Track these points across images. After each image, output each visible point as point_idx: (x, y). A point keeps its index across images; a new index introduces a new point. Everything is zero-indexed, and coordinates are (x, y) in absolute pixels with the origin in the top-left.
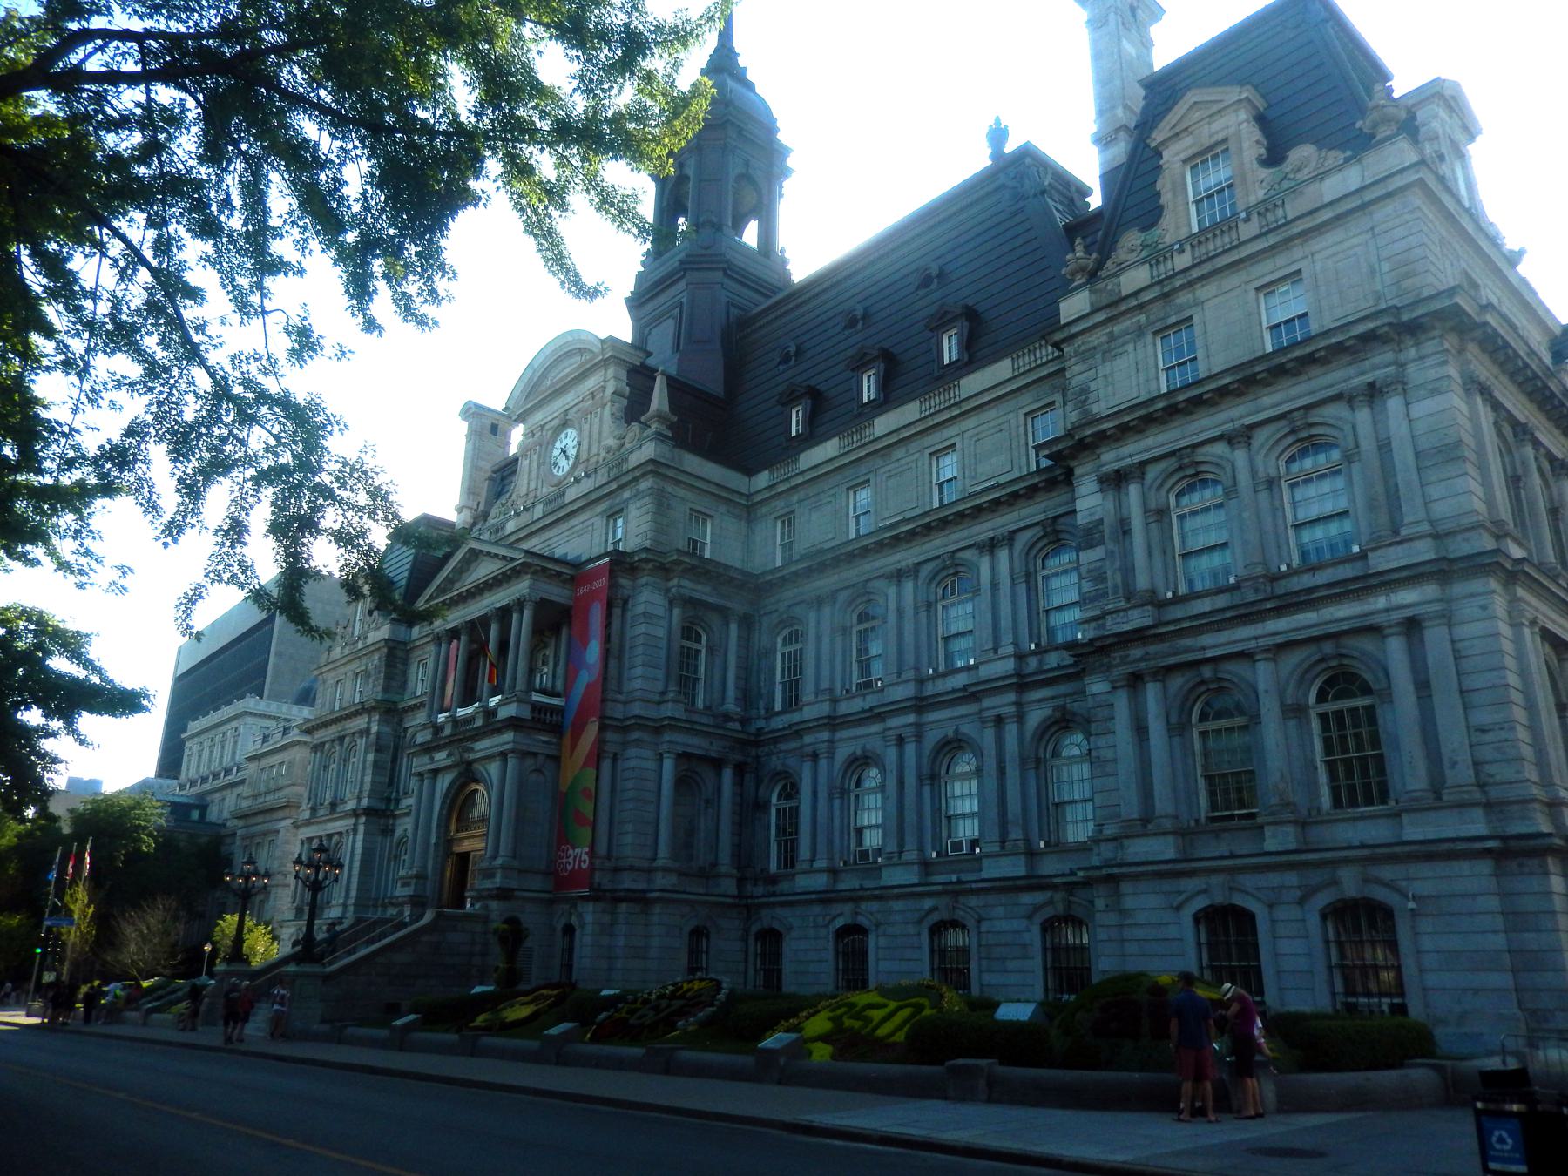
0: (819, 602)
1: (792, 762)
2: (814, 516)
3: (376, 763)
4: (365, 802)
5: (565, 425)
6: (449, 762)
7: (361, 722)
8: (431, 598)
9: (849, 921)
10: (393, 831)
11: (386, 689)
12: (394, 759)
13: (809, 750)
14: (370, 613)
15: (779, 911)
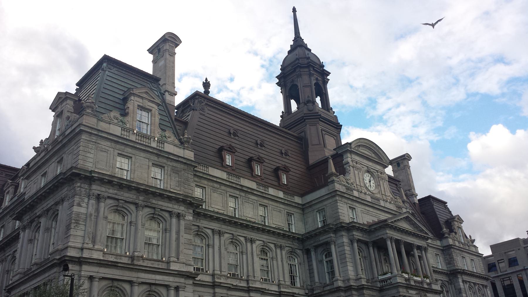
5: (368, 172)
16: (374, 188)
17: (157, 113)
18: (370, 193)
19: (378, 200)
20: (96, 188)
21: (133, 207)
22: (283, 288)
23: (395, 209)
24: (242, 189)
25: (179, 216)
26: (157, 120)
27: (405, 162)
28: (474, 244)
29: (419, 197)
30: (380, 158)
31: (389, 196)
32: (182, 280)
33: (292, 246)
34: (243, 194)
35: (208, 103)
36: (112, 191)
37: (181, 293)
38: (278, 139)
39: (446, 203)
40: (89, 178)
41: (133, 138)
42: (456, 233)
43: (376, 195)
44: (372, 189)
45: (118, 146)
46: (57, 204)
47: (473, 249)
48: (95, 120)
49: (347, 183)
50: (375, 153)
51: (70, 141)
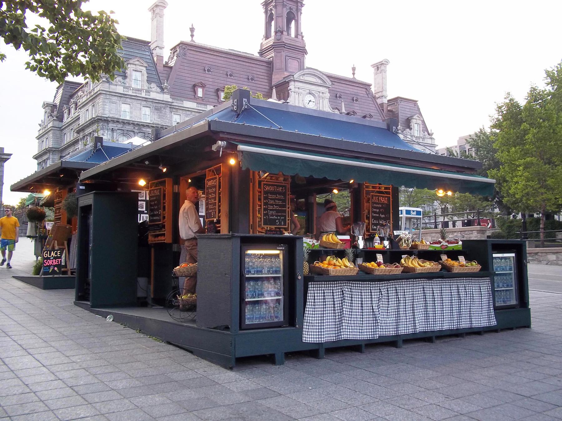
17: (145, 73)
20: (111, 125)
21: (132, 133)
26: (146, 78)
27: (383, 67)
28: (433, 136)
29: (388, 98)
36: (120, 126)
39: (417, 101)
40: (106, 121)
41: (130, 93)
42: (411, 129)
45: (122, 99)
46: (93, 131)
47: (429, 141)
48: (107, 85)
50: (319, 78)
51: (96, 96)
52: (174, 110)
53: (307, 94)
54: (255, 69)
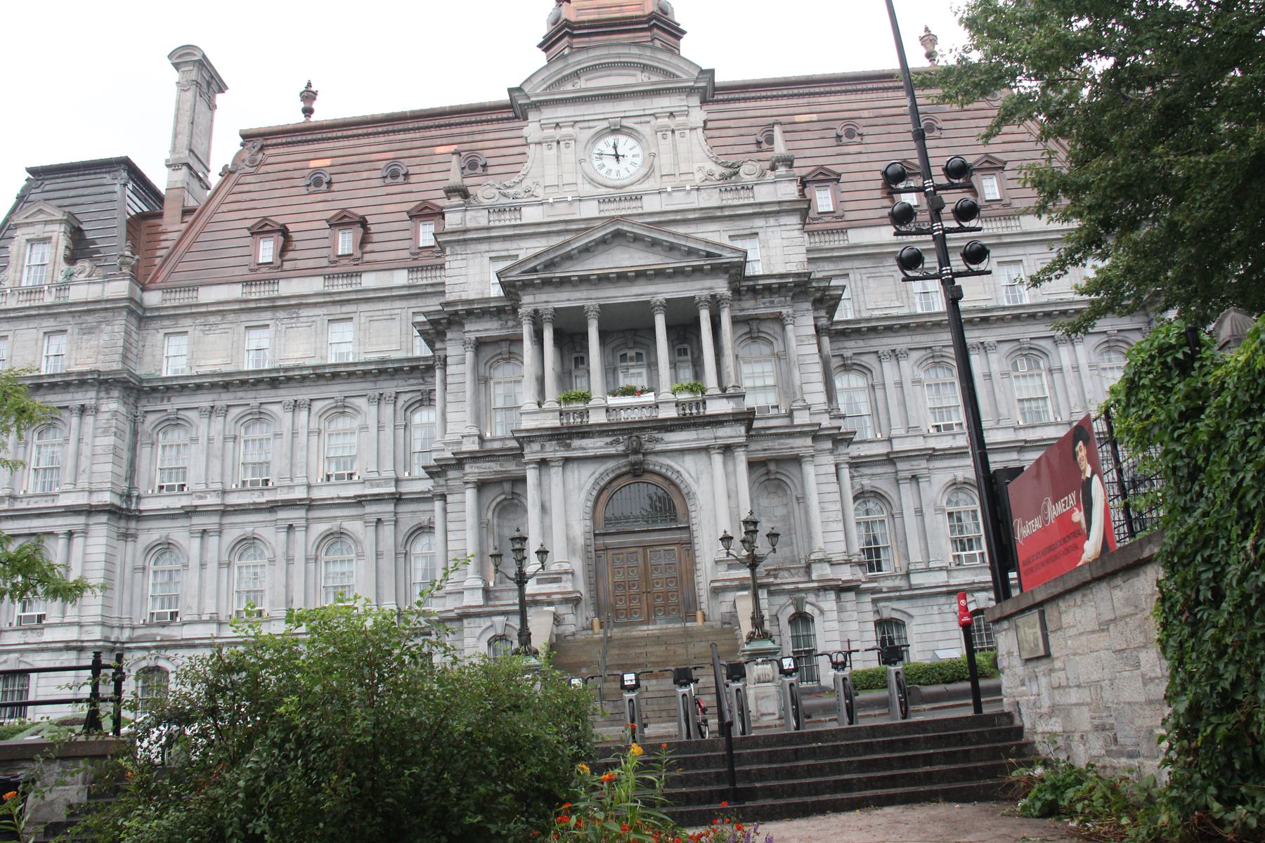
0: (895, 355)
1: (883, 485)
2: (872, 283)
3: (115, 447)
4: (107, 498)
5: (615, 131)
6: (612, 450)
7: (87, 397)
8: (534, 270)
9: (982, 606)
10: (135, 536)
11: (125, 358)
12: (133, 449)
13: (908, 475)
14: (71, 260)
15: (896, 605)
16: (632, 169)
18: (603, 190)
19: (638, 198)
22: (372, 486)
23: (715, 202)
24: (273, 306)
25: (83, 410)
30: (667, 73)
31: (700, 169)
32: (81, 520)
33: (422, 387)
34: (281, 314)
35: (269, 142)
37: (78, 542)
38: (468, 134)
43: (633, 188)
44: (624, 174)
49: (505, 195)
50: (645, 68)
52: (166, 323)
53: (599, 135)
54: (491, 136)
